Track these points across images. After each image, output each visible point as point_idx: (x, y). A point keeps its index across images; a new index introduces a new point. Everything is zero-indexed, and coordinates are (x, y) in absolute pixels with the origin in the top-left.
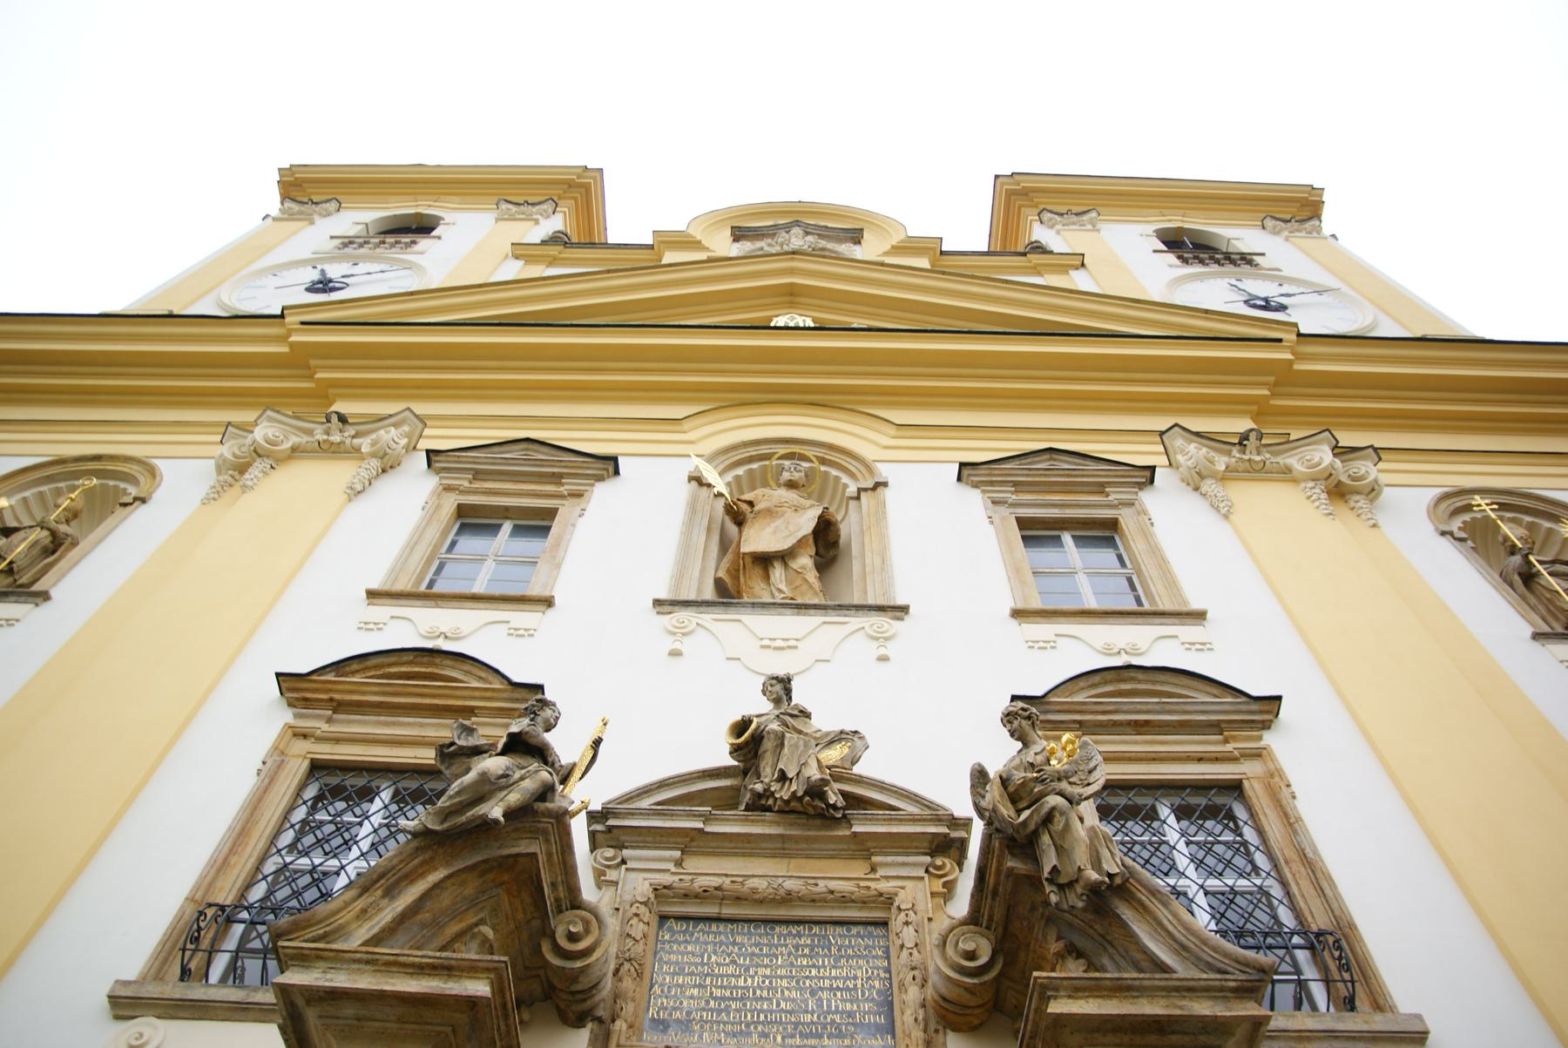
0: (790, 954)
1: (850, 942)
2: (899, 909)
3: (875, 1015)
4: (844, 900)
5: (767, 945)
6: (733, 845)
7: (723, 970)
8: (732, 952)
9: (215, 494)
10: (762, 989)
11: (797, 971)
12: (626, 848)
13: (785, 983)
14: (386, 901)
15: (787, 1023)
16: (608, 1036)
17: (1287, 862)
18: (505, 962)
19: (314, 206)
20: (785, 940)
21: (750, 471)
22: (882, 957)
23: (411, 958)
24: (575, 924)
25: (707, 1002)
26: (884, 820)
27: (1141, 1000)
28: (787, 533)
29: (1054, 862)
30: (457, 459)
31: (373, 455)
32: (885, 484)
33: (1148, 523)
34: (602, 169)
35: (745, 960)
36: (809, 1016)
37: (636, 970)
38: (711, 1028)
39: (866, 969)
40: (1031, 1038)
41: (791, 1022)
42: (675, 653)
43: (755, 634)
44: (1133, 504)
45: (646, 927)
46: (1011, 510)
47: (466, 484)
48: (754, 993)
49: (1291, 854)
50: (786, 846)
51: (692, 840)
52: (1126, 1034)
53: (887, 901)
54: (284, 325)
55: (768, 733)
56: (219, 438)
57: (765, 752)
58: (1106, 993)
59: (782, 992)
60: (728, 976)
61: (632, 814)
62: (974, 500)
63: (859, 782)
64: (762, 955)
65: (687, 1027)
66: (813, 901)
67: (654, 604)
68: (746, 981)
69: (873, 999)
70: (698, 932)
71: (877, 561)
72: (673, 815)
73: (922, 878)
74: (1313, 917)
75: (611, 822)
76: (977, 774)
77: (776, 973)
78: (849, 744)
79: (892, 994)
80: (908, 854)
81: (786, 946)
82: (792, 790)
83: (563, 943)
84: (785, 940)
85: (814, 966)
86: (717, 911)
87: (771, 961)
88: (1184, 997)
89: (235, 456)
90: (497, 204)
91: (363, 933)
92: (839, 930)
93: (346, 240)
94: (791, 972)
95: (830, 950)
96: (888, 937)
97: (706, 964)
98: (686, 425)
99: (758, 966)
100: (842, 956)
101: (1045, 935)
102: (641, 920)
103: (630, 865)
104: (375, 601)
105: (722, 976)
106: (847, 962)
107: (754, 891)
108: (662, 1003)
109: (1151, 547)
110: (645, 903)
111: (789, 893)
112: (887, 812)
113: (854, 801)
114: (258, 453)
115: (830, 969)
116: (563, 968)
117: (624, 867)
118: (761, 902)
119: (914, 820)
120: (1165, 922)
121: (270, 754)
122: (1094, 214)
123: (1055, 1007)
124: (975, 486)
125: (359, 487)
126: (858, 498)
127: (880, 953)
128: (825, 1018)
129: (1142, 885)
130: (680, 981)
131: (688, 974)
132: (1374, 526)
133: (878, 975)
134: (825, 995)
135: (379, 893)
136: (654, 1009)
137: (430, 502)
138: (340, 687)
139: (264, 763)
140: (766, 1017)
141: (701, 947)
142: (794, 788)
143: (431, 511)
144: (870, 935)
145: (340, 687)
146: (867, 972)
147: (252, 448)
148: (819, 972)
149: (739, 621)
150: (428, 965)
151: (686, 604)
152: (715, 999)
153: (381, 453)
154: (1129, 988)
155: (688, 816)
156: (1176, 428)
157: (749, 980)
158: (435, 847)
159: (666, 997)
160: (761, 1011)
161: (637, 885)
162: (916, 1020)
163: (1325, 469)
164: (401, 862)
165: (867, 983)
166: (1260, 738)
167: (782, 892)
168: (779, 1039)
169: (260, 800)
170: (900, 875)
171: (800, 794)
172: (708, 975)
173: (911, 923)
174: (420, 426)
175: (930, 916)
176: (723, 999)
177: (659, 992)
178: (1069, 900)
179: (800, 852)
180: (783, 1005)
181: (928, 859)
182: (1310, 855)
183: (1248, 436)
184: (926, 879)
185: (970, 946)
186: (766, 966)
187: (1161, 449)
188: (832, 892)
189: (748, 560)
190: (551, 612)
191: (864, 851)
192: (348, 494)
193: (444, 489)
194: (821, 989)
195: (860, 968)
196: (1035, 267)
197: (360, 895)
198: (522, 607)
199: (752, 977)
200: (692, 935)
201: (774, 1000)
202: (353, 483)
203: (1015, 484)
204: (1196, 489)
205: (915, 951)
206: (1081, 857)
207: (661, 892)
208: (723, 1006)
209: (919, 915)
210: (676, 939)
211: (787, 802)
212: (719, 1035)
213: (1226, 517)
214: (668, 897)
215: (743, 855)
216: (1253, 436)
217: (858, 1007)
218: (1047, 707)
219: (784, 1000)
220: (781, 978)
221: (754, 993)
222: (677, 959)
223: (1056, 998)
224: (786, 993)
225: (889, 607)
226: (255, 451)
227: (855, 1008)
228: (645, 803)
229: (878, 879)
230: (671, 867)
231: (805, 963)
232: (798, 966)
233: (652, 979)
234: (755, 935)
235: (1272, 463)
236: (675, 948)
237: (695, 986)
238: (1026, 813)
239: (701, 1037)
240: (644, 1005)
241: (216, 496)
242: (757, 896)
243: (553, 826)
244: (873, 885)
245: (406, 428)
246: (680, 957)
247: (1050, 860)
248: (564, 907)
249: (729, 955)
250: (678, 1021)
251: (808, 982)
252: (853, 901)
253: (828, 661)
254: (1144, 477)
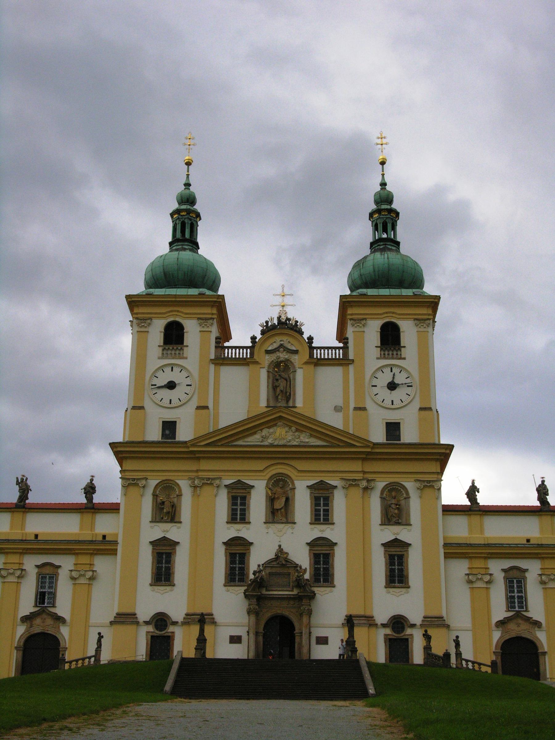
53: (290, 573)
62: (308, 491)
151: (268, 523)
196: (341, 364)
207: (269, 572)
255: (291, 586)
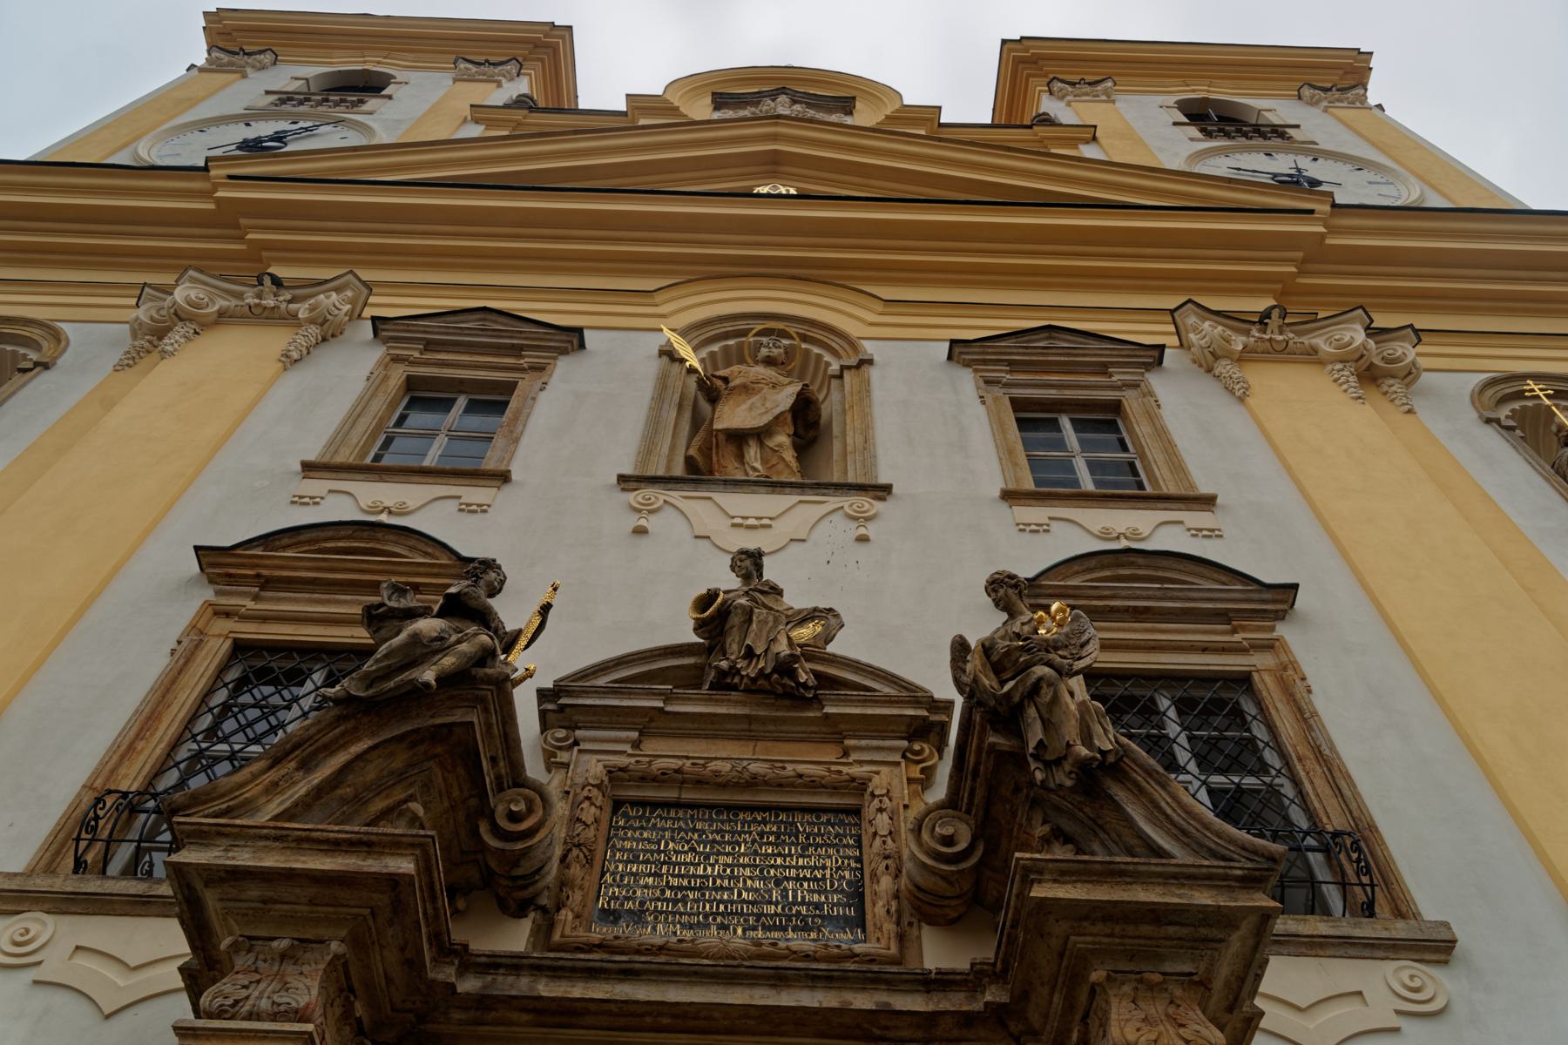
0: (754, 841)
1: (819, 829)
2: (873, 795)
3: (844, 906)
4: (814, 785)
5: (729, 832)
6: (696, 726)
7: (681, 858)
8: (691, 839)
9: (130, 361)
10: (722, 878)
11: (761, 860)
12: (580, 728)
13: (748, 872)
14: (301, 773)
15: (749, 915)
16: (551, 926)
17: (1300, 760)
18: (432, 837)
19: (246, 57)
20: (749, 827)
21: (726, 348)
22: (853, 846)
23: (325, 834)
24: (517, 802)
25: (663, 892)
26: (859, 701)
27: (1134, 886)
28: (763, 410)
29: (1040, 736)
30: (406, 328)
31: (312, 321)
32: (870, 362)
33: (1154, 404)
34: (571, 27)
35: (705, 848)
36: (773, 907)
37: (585, 856)
38: (666, 919)
39: (836, 859)
40: (1012, 927)
41: (753, 914)
42: (640, 531)
43: (728, 514)
44: (1138, 386)
45: (598, 812)
46: (1005, 390)
47: (417, 354)
48: (714, 882)
49: (1303, 750)
50: (753, 727)
51: (651, 720)
52: (1117, 923)
54: (208, 179)
55: (736, 608)
56: (133, 301)
57: (731, 628)
58: (1095, 878)
59: (745, 881)
60: (686, 864)
61: (585, 692)
62: (966, 381)
63: (833, 662)
64: (724, 842)
65: (640, 918)
66: (781, 785)
67: (618, 480)
68: (705, 869)
69: (843, 890)
70: (656, 818)
71: (859, 439)
72: (630, 694)
73: (898, 764)
74: (1328, 817)
75: (564, 701)
76: (959, 647)
77: (738, 861)
78: (823, 622)
79: (863, 885)
80: (883, 738)
81: (750, 833)
82: (760, 667)
83: (504, 824)
84: (749, 827)
85: (779, 854)
86: (676, 796)
87: (733, 849)
88: (1184, 885)
89: (152, 319)
90: (454, 63)
91: (274, 807)
92: (807, 817)
93: (284, 96)
94: (755, 860)
95: (797, 839)
96: (860, 825)
97: (662, 851)
98: (659, 298)
99: (719, 853)
100: (810, 845)
101: (1029, 820)
102: (592, 804)
103: (583, 746)
104: (311, 474)
105: (680, 864)
106: (816, 850)
107: (717, 773)
108: (614, 893)
109: (1156, 429)
110: (598, 787)
111: (754, 776)
112: (862, 693)
113: (825, 681)
114: (179, 316)
115: (797, 858)
116: (503, 850)
117: (576, 748)
118: (724, 786)
119: (889, 701)
120: (1163, 804)
121: (186, 633)
122: (1109, 84)
123: (1038, 892)
124: (967, 364)
125: (295, 355)
126: (841, 377)
127: (851, 842)
128: (790, 909)
129: (1137, 765)
130: (634, 869)
131: (643, 862)
132: (1410, 411)
133: (849, 865)
134: (790, 885)
135: (293, 764)
136: (604, 899)
137: (376, 373)
138: (268, 562)
139: (179, 642)
140: (726, 908)
141: (657, 833)
142: (761, 665)
143: (376, 382)
144: (841, 824)
145: (268, 562)
146: (837, 862)
147: (172, 311)
148: (785, 861)
149: (710, 498)
150: (345, 840)
152: (672, 888)
153: (320, 321)
154: (1122, 873)
155: (647, 694)
156: (1189, 305)
157: (709, 869)
158: (359, 716)
159: (618, 886)
160: (721, 901)
161: (592, 767)
162: (888, 912)
163: (1357, 348)
164: (319, 731)
165: (836, 873)
166: (1272, 629)
167: (746, 775)
168: (740, 931)
169: (173, 682)
170: (875, 759)
171: (768, 671)
172: (664, 863)
173: (885, 810)
174: (365, 291)
175: (906, 802)
176: (681, 888)
177: (610, 880)
178: (1056, 777)
179: (767, 734)
180: (745, 895)
181: (905, 743)
182: (1327, 752)
183: (1270, 313)
184: (903, 765)
185: (948, 831)
186: (728, 854)
187: (1172, 328)
188: (800, 776)
189: (722, 437)
190: (506, 489)
191: (837, 733)
192: (283, 362)
193: (392, 360)
194: (787, 879)
195: (830, 857)
197: (271, 767)
198: (475, 482)
199: (713, 866)
200: (648, 821)
201: (736, 891)
202: (289, 351)
203: (1011, 363)
204: (1209, 370)
205: (889, 840)
206: (1071, 731)
208: (679, 896)
209: (894, 802)
210: (631, 825)
211: (754, 680)
212: (675, 926)
213: (1241, 400)
214: (623, 780)
215: (707, 737)
216: (1275, 313)
217: (827, 898)
218: (1038, 591)
219: (747, 890)
220: (744, 866)
221: (714, 882)
222: (632, 846)
223: (1040, 881)
224: (749, 882)
225: (870, 486)
226: (176, 314)
227: (823, 899)
228: (602, 681)
229: (850, 764)
230: (627, 748)
231: (770, 851)
232: (762, 855)
233: (603, 868)
234: (717, 821)
235: (1295, 343)
236: (629, 835)
237: (650, 875)
238: (1011, 684)
239: (654, 928)
240: (593, 894)
241: (131, 362)
242: (720, 780)
243: (492, 694)
244: (845, 769)
245: (349, 293)
246: (635, 844)
247: (1035, 734)
248: (506, 785)
249: (688, 842)
250: (630, 911)
251: (772, 872)
252: (823, 786)
253: (804, 541)
254: (1151, 356)
255: (877, 910)
